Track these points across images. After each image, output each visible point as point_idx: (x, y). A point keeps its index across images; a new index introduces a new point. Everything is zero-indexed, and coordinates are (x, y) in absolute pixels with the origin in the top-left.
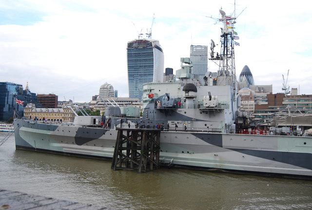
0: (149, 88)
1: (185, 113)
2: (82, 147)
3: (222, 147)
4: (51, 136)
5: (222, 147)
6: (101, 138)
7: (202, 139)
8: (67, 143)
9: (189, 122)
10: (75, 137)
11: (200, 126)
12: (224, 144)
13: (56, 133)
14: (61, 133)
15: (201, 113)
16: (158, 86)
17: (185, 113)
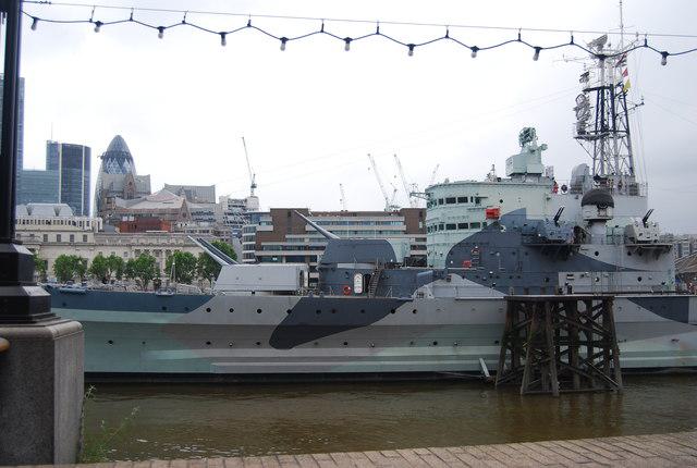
0: (474, 195)
1: (597, 254)
2: (295, 352)
3: (686, 322)
4: (164, 328)
5: (686, 322)
6: (381, 322)
7: (651, 309)
9: (606, 274)
10: (279, 327)
11: (627, 281)
12: (690, 319)
13: (198, 316)
14: (220, 317)
15: (629, 254)
16: (498, 190)
17: (597, 254)
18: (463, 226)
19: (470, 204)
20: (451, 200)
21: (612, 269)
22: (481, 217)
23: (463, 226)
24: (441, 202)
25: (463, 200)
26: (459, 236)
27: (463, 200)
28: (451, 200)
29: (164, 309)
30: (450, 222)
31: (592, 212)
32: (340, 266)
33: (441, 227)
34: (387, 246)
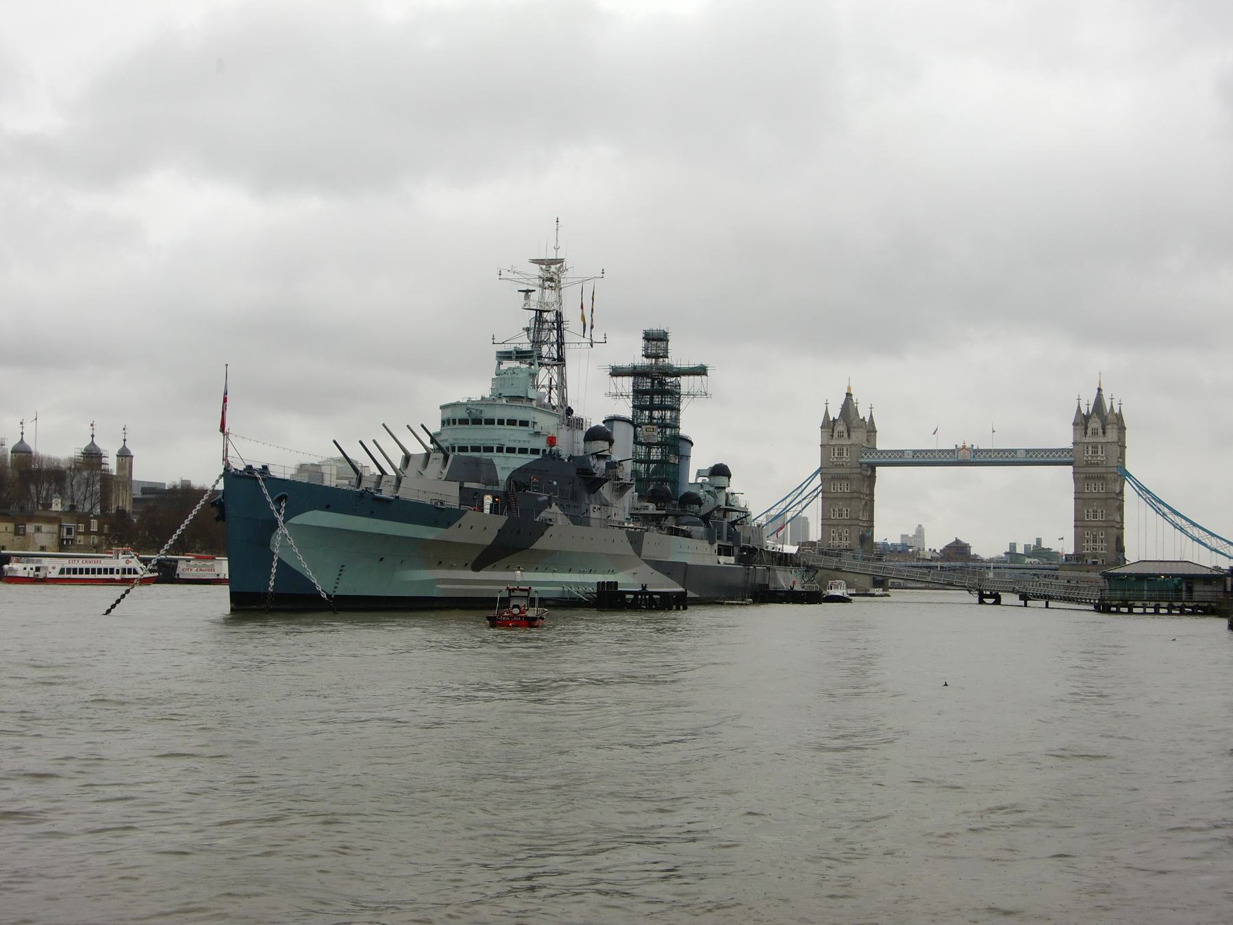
2: (483, 575)
8: (451, 567)
13: (451, 534)
18: (523, 451)
19: (530, 427)
20: (512, 422)
21: (607, 505)
22: (541, 444)
23: (523, 451)
24: (501, 422)
25: (524, 423)
26: (518, 461)
27: (524, 423)
28: (512, 422)
29: (436, 523)
30: (511, 445)
31: (601, 446)
32: (467, 485)
33: (500, 450)
34: (491, 464)
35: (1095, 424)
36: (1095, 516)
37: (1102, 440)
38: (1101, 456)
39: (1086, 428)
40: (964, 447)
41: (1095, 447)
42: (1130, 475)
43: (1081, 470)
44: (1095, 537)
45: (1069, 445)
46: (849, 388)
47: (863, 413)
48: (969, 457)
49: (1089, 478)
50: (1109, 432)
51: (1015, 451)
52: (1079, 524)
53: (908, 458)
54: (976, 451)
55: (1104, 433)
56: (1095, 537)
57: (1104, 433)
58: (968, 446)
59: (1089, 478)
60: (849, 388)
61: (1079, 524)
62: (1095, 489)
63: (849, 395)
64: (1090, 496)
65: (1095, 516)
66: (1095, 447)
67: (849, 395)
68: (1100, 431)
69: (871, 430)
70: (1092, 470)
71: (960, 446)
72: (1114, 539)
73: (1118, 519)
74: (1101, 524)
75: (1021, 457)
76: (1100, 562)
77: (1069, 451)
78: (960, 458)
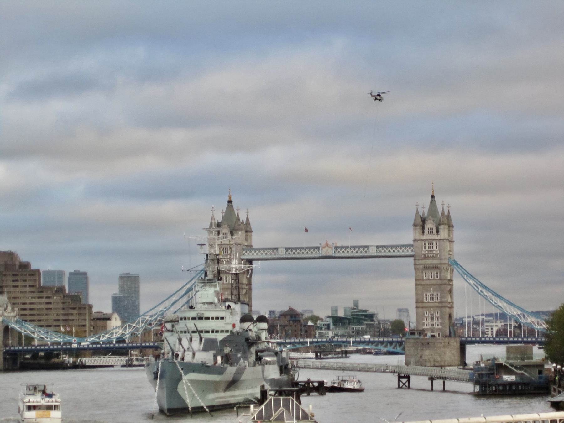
35: (430, 225)
36: (432, 298)
37: (436, 237)
38: (436, 251)
39: (423, 228)
40: (327, 245)
41: (431, 244)
42: (457, 264)
43: (421, 262)
44: (432, 315)
45: (410, 242)
46: (230, 197)
47: (243, 218)
48: (331, 252)
49: (426, 268)
50: (441, 231)
51: (368, 247)
52: (420, 305)
53: (282, 253)
54: (336, 248)
55: (438, 232)
56: (432, 315)
57: (438, 232)
58: (330, 243)
59: (426, 268)
60: (230, 197)
61: (420, 305)
62: (430, 276)
63: (230, 202)
64: (428, 282)
65: (432, 298)
66: (431, 244)
67: (230, 202)
68: (435, 231)
69: (248, 231)
70: (429, 262)
71: (324, 244)
72: (447, 317)
73: (449, 300)
74: (437, 304)
75: (373, 251)
76: (436, 334)
77: (410, 246)
78: (324, 254)
